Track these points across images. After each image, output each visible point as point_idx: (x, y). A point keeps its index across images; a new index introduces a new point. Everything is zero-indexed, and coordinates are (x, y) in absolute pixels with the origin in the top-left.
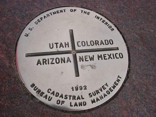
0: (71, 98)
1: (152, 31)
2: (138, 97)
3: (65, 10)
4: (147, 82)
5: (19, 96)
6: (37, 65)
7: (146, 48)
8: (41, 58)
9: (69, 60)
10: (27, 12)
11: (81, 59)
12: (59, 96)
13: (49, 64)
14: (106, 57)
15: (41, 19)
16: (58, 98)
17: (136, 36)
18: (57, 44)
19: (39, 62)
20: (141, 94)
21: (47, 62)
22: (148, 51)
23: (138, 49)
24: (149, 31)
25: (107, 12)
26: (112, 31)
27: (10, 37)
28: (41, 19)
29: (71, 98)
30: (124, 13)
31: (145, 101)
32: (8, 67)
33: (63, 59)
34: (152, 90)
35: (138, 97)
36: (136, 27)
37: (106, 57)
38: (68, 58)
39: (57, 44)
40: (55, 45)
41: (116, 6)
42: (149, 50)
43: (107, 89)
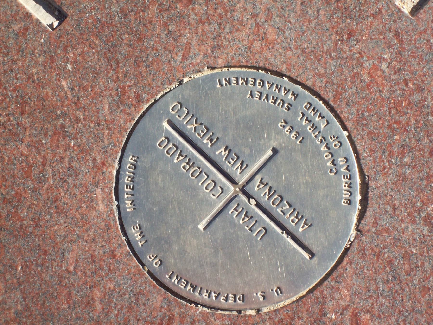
1: (64, 83)
2: (227, 29)
4: (187, 31)
5: (379, 207)
7: (117, 73)
20: (220, 28)
22: (121, 65)
23: (134, 85)
25: (100, 198)
27: (305, 315)
30: (70, 164)
31: (226, 15)
32: (353, 266)
34: (196, 15)
35: (227, 29)
36: (85, 119)
41: (65, 194)
42: (118, 64)
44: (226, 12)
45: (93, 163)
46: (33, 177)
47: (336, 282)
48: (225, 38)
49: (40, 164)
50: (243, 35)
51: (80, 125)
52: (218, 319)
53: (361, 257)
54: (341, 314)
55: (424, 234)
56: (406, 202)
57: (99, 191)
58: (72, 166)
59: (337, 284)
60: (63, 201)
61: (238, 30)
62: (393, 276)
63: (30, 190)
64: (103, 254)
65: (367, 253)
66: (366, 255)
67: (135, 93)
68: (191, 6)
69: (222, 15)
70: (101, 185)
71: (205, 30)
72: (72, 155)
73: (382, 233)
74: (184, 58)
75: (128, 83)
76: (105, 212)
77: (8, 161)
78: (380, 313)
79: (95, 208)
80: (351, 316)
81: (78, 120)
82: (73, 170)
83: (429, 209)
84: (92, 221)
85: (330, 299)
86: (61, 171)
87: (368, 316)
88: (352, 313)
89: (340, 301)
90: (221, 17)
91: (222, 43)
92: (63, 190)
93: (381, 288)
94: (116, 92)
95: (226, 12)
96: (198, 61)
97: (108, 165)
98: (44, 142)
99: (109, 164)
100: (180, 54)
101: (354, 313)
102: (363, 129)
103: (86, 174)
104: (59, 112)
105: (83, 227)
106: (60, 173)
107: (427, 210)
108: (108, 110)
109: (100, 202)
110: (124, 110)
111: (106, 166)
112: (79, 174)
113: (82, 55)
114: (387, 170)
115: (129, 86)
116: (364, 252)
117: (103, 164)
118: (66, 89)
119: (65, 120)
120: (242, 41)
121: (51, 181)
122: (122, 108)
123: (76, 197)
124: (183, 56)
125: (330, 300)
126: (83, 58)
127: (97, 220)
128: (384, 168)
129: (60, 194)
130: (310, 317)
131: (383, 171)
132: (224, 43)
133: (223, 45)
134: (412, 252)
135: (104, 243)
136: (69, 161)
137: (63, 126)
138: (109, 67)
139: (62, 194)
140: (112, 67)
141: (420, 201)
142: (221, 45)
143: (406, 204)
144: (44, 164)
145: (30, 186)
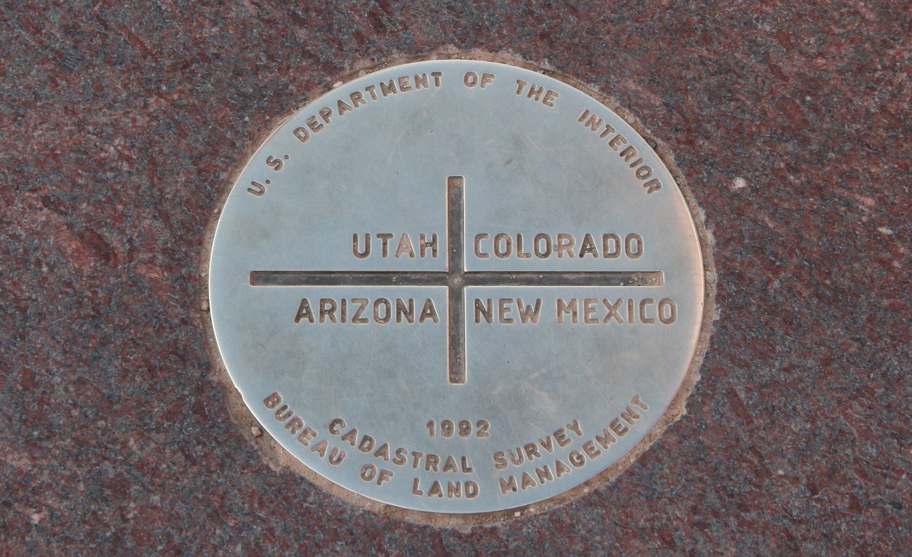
0: (421, 461)
1: (870, 201)
3: (436, 74)
4: (770, 438)
6: (297, 319)
7: (808, 286)
8: (314, 293)
9: (428, 311)
11: (484, 312)
12: (374, 449)
13: (343, 320)
14: (508, 309)
15: (325, 114)
16: (368, 457)
17: (771, 225)
18: (385, 237)
19: (303, 312)
21: (337, 314)
22: (815, 301)
24: (848, 204)
25: (645, 95)
26: (650, 191)
28: (325, 114)
29: (421, 461)
30: (738, 100)
31: (737, 517)
32: (176, 321)
33: (407, 306)
36: (783, 178)
37: (508, 309)
38: (428, 304)
39: (385, 237)
40: (376, 244)
42: (820, 297)
43: (575, 442)
44: (742, 522)
45: (706, 131)
46: (773, 39)
47: (182, 277)
48: (701, 479)
49: (780, 64)
50: (679, 512)
51: (782, 165)
52: (308, 81)
53: (176, 344)
54: (130, 241)
55: (107, 462)
56: (179, 484)
57: (657, 101)
58: (732, 100)
59: (177, 275)
60: (694, 44)
61: (694, 510)
62: (100, 358)
63: (757, 19)
65: (173, 357)
66: (172, 353)
67: (751, 280)
68: (804, 481)
69: (742, 511)
70: (662, 112)
71: (744, 465)
72: (747, 116)
73: (174, 406)
74: (732, 393)
75: (776, 284)
77: (830, 30)
78: (70, 291)
79: (638, 75)
80: (113, 248)
82: (725, 97)
83: (132, 505)
84: (624, 55)
85: (169, 245)
86: (740, 80)
87: (86, 270)
88: (115, 255)
90: (743, 507)
91: (698, 469)
92: (710, 60)
93: (103, 326)
94: (779, 257)
95: (742, 522)
96: (706, 409)
99: (681, 150)
100: (742, 395)
101: (112, 256)
102: (352, 534)
103: (701, 108)
104: (832, 155)
105: (630, 35)
106: (739, 77)
107: (135, 501)
108: (763, 221)
109: (639, 88)
110: (740, 240)
111: (684, 143)
112: (710, 99)
113: (886, 265)
114: (256, 505)
115: (769, 281)
116: (177, 354)
117: (690, 142)
118: (857, 196)
119: (811, 152)
120: (671, 500)
121: (738, 55)
122: (746, 241)
123: (682, 65)
124: (736, 395)
125: (167, 244)
126: (881, 261)
127: (618, 62)
128: (261, 503)
129: (708, 50)
130: (175, 196)
131: (261, 498)
132: (694, 472)
133: (693, 467)
134: (102, 418)
135: (577, 40)
136: (744, 104)
137: (805, 141)
138: (828, 282)
139: (705, 53)
140: (825, 285)
141: (159, 505)
142: (696, 463)
143: (178, 480)
145: (762, 23)
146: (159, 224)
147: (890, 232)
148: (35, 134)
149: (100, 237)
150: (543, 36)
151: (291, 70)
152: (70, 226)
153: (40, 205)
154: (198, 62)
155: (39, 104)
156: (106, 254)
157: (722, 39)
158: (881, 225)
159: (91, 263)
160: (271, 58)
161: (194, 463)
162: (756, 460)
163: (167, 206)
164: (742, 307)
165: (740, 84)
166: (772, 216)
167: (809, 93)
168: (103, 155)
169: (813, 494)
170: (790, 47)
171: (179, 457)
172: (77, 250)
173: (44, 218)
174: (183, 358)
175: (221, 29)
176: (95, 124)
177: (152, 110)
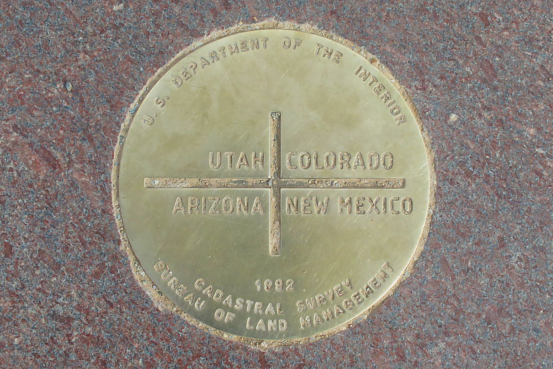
7: (493, 188)
10: (152, 41)
30: (454, 60)
55: (58, 305)
61: (418, 336)
64: (345, 5)
66: (96, 233)
76: (380, 46)
77: (513, 12)
78: (32, 190)
80: (58, 161)
81: (488, 109)
85: (93, 159)
89: (82, 165)
97: (419, 91)
98: (497, 59)
105: (388, 13)
108: (467, 144)
111: (420, 89)
116: (99, 234)
117: (424, 89)
138: (505, 186)
144: (478, 38)
146: (86, 145)
147: (542, 152)
148: (7, 80)
149: (49, 153)
150: (333, 12)
151: (170, 35)
152: (31, 145)
153: (11, 130)
154: (110, 29)
155: (8, 58)
156: (54, 164)
157: (446, 17)
158: (538, 147)
159: (44, 171)
160: (158, 26)
161: (112, 306)
162: (456, 303)
163: (91, 131)
164: (452, 202)
165: (455, 49)
166: (473, 141)
167: (498, 56)
168: (50, 95)
169: (488, 324)
170: (487, 24)
171: (102, 302)
172: (35, 162)
173: (13, 139)
174: (103, 237)
175: (125, 6)
176: (45, 73)
177: (80, 63)
